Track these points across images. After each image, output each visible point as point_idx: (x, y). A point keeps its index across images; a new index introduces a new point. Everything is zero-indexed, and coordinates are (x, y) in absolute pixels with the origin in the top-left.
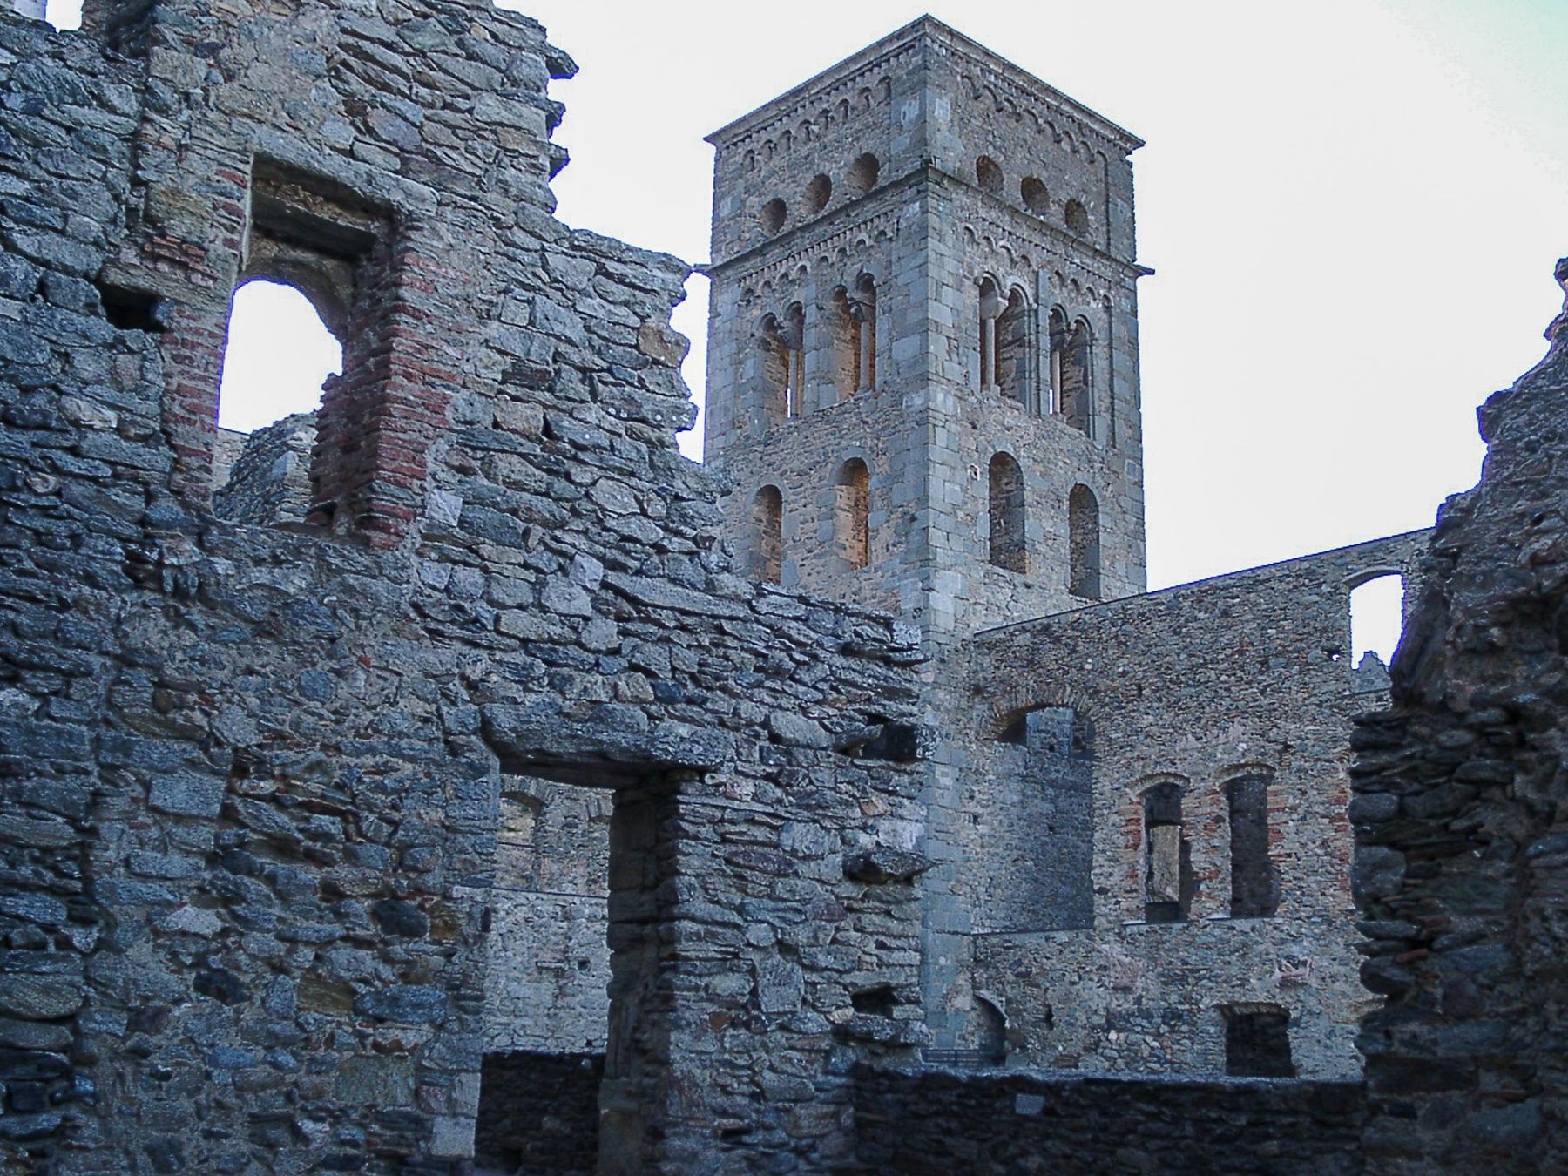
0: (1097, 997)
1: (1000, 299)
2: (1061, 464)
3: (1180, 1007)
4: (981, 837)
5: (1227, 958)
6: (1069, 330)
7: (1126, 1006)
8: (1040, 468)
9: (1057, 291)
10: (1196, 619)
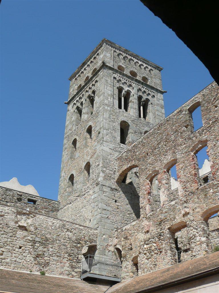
0: (142, 236)
4: (118, 206)
5: (170, 213)
10: (158, 132)
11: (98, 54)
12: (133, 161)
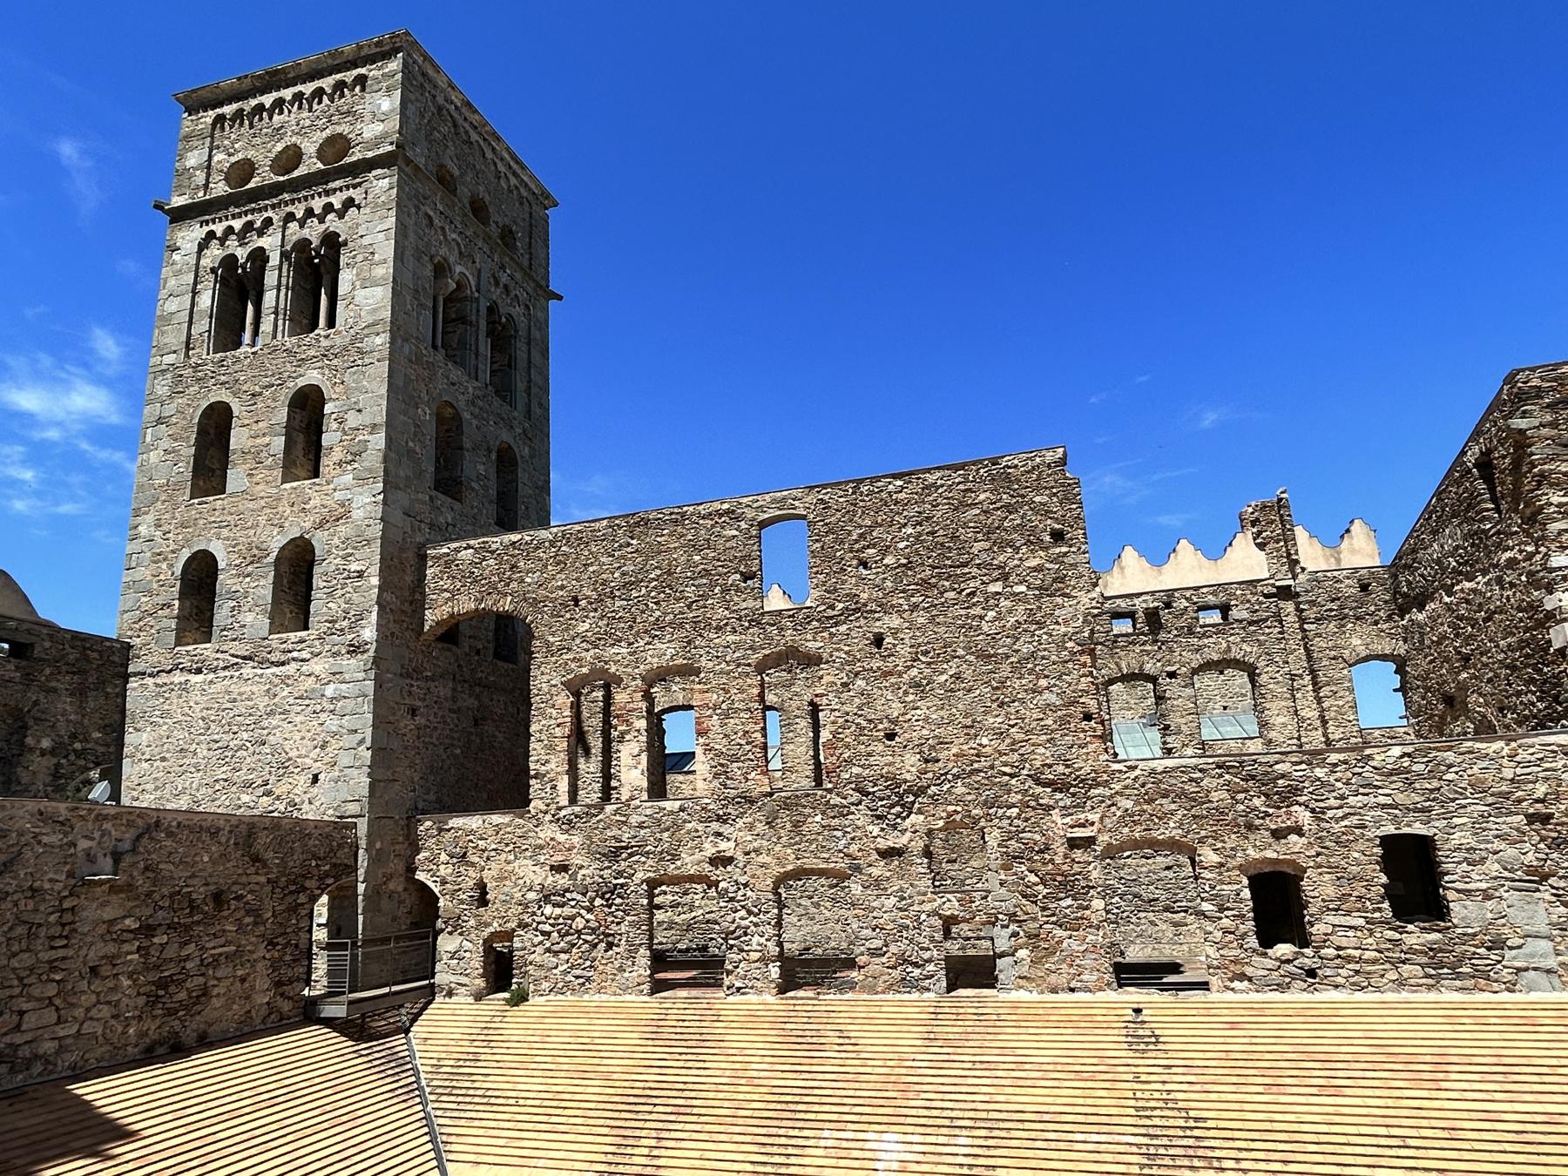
0: (533, 873)
1: (450, 281)
2: (491, 423)
3: (615, 882)
5: (658, 835)
6: (500, 323)
7: (563, 881)
8: (475, 422)
9: (493, 289)
10: (629, 545)
11: (361, 80)
12: (509, 598)
